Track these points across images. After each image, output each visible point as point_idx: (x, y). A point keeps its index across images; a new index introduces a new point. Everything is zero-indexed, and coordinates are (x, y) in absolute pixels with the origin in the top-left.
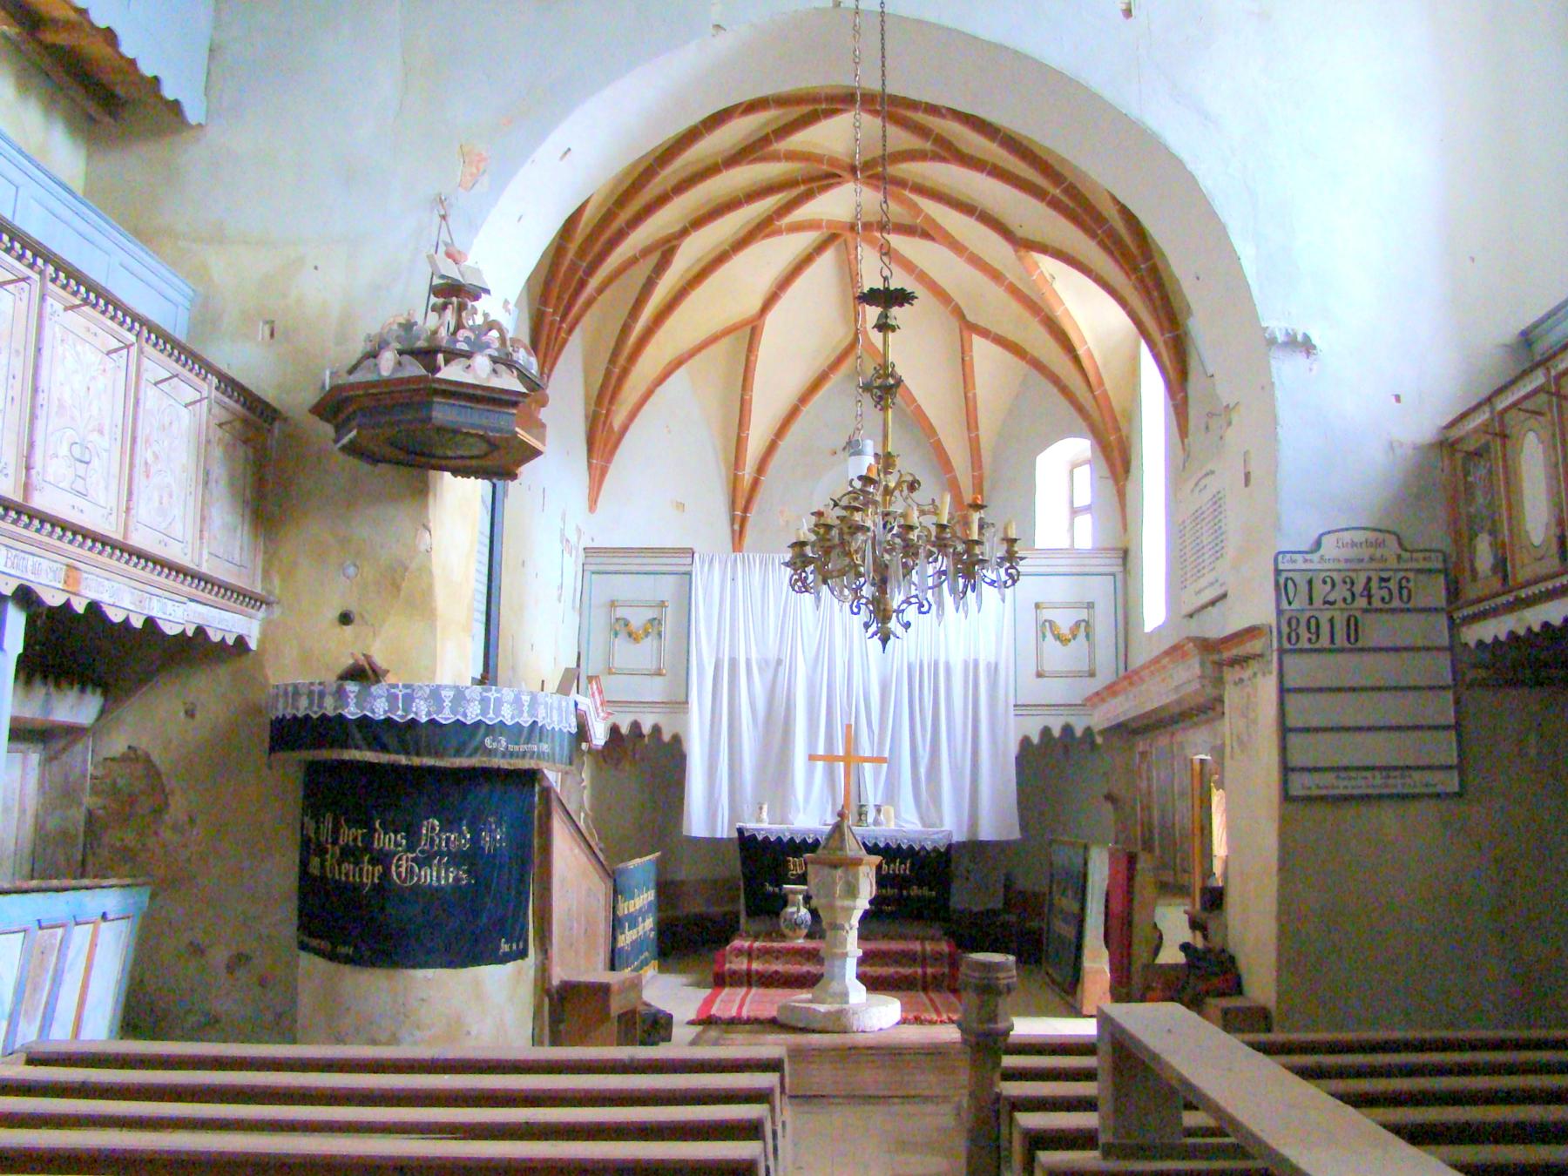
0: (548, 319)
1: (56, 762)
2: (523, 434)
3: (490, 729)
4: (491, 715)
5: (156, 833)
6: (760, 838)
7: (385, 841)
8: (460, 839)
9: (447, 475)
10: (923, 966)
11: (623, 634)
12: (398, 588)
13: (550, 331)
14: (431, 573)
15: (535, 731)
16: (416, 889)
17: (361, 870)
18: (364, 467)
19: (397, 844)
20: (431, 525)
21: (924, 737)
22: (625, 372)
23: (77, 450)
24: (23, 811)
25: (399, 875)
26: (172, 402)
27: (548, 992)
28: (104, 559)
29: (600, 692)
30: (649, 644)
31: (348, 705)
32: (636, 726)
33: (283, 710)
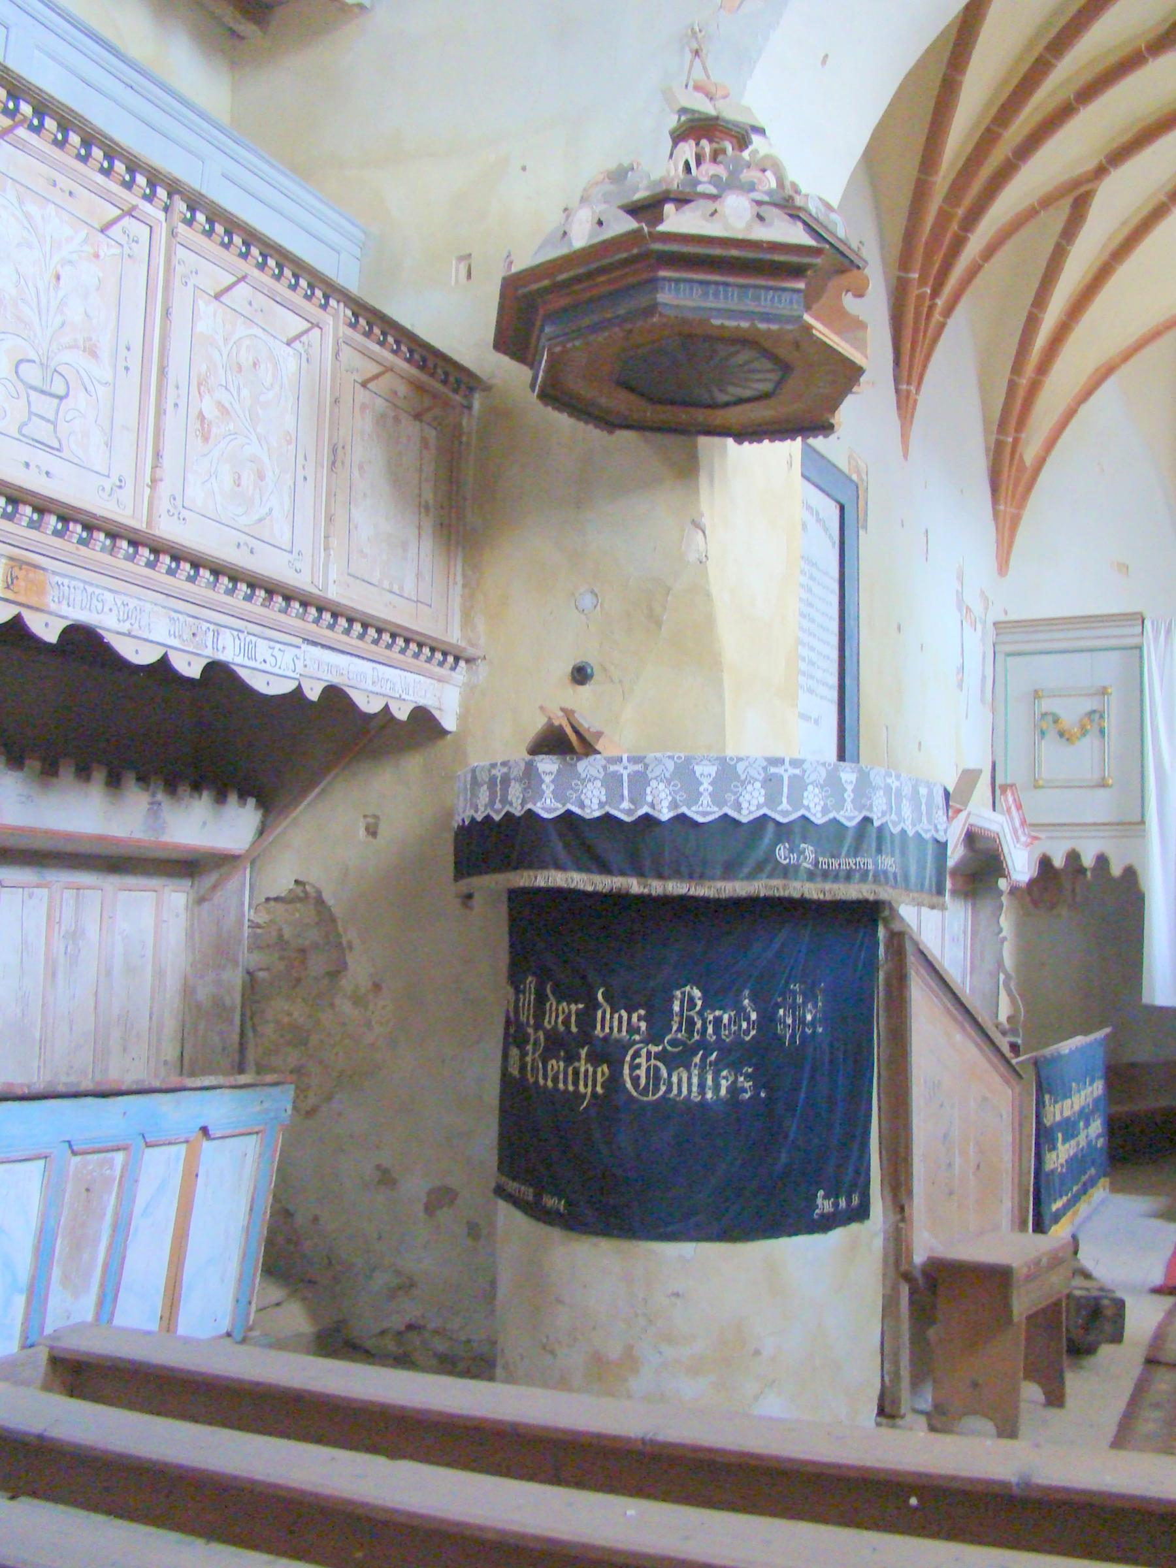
0: (914, 292)
1: (206, 905)
2: (822, 331)
3: (784, 831)
4: (785, 805)
5: (332, 1005)
7: (613, 1023)
8: (739, 1020)
9: (730, 441)
11: (1052, 735)
12: (659, 624)
13: (917, 314)
14: (708, 595)
15: (867, 834)
16: (667, 1109)
17: (576, 1073)
18: (593, 434)
19: (632, 1030)
20: (705, 521)
22: (1034, 388)
23: (31, 373)
24: (159, 974)
25: (635, 1080)
26: (255, 331)
27: (907, 1277)
28: (159, 576)
29: (1019, 807)
30: (1087, 744)
31: (541, 795)
32: (1073, 857)
33: (464, 814)
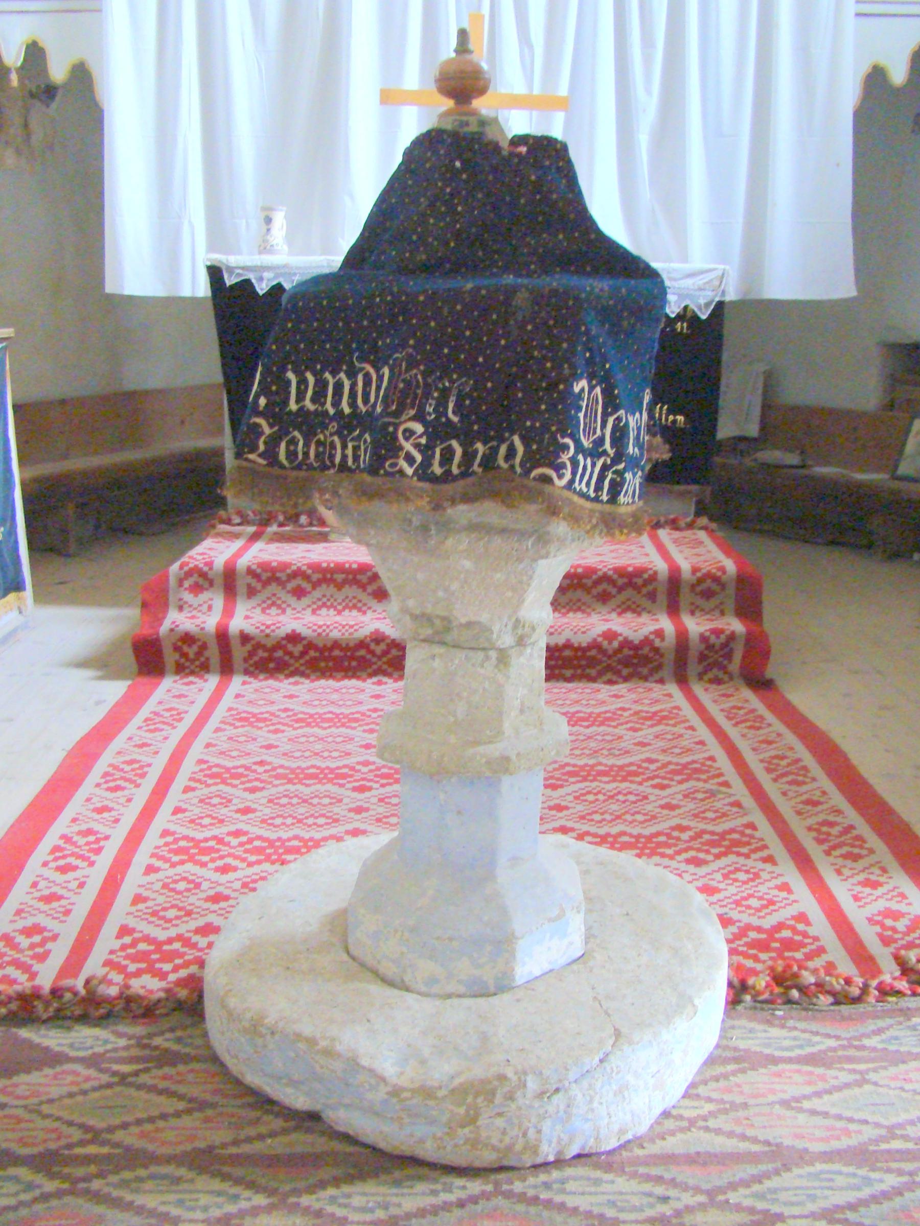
6: (262, 288)
10: (673, 610)
21: (648, 61)
